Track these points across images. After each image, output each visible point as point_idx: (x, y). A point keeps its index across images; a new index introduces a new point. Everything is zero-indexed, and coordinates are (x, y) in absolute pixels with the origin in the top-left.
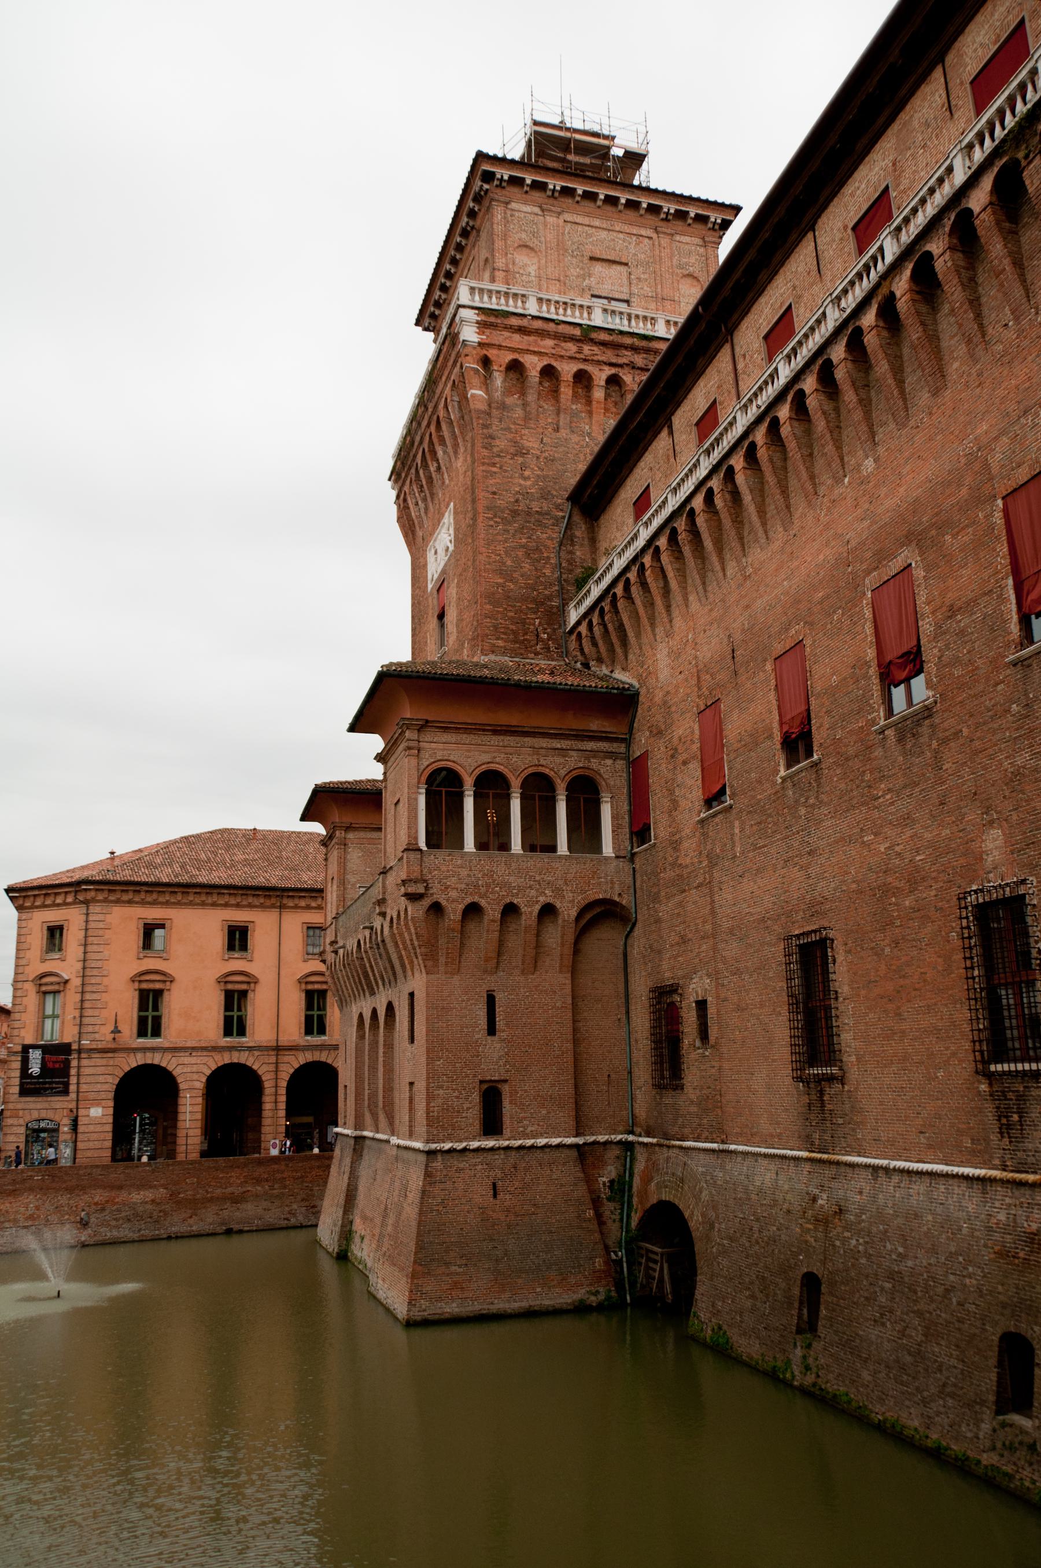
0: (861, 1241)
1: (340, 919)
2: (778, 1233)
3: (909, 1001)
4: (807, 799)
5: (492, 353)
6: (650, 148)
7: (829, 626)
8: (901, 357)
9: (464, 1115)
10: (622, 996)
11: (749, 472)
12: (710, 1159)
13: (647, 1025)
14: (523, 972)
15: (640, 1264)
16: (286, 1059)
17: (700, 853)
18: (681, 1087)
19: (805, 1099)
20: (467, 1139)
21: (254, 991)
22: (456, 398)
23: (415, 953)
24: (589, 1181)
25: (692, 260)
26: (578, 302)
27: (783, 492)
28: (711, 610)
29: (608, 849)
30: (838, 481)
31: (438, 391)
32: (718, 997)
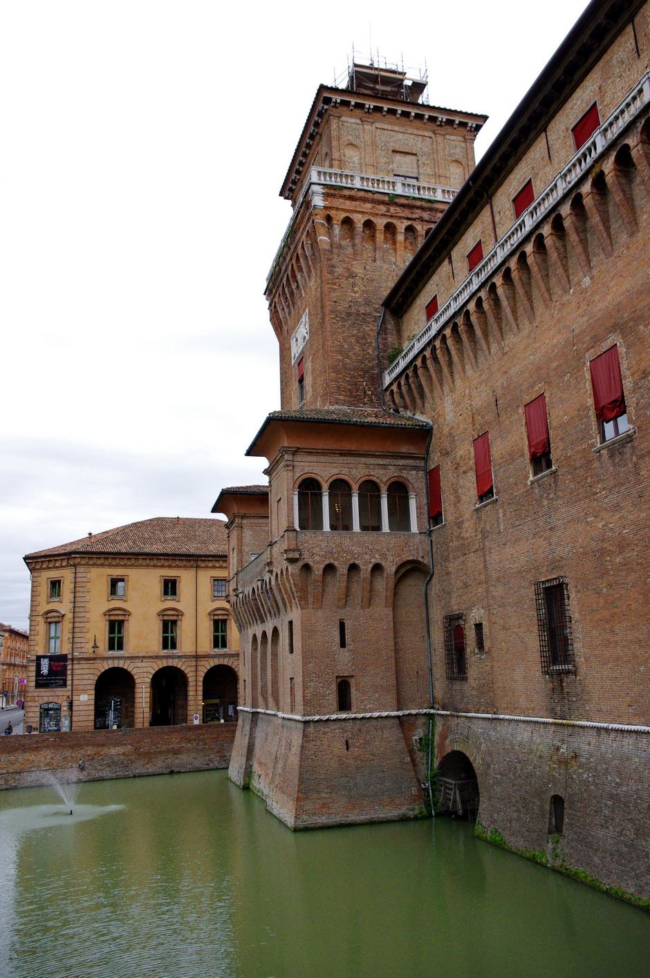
0: (590, 775)
1: (240, 575)
2: (534, 770)
3: (620, 623)
4: (548, 495)
5: (332, 213)
6: (428, 80)
7: (561, 384)
8: (608, 212)
9: (327, 698)
10: (425, 621)
11: (505, 286)
12: (485, 723)
13: (442, 639)
14: (362, 607)
15: (440, 791)
16: (202, 663)
17: (476, 530)
18: (466, 679)
19: (551, 685)
20: (329, 713)
21: (181, 620)
22: (310, 242)
23: (293, 596)
24: (407, 739)
25: (458, 151)
26: (386, 179)
27: (529, 299)
28: (481, 375)
29: (414, 528)
30: (566, 291)
31: (297, 238)
32: (490, 621)
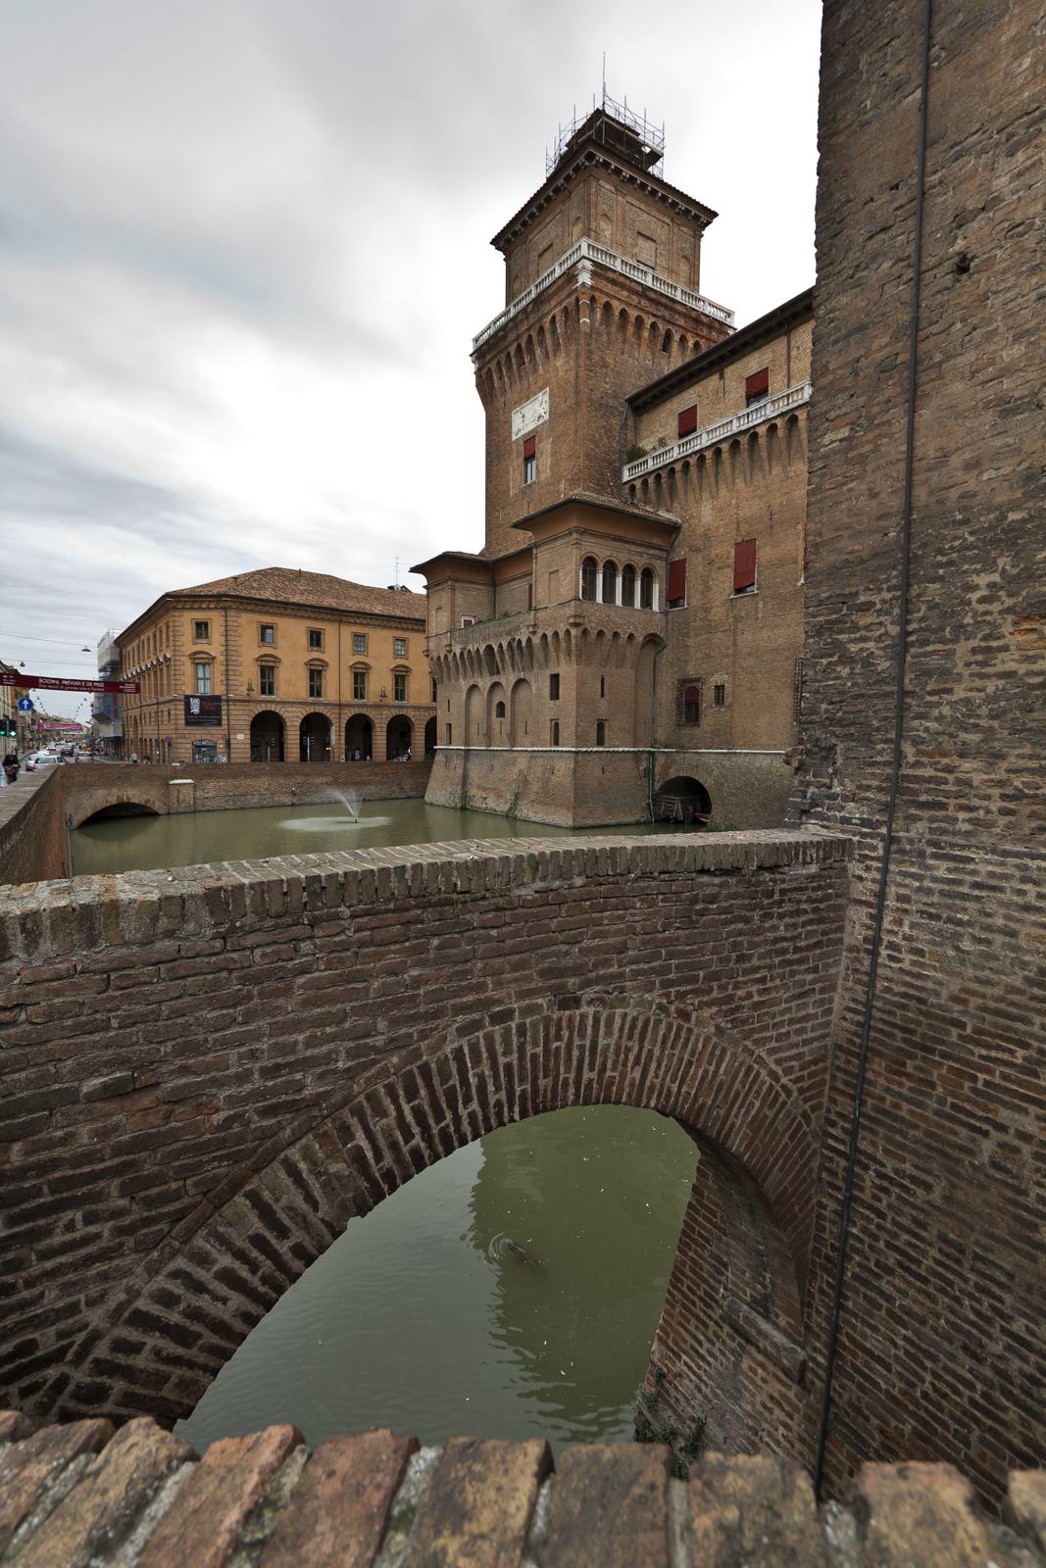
5: (597, 294)
6: (665, 152)
